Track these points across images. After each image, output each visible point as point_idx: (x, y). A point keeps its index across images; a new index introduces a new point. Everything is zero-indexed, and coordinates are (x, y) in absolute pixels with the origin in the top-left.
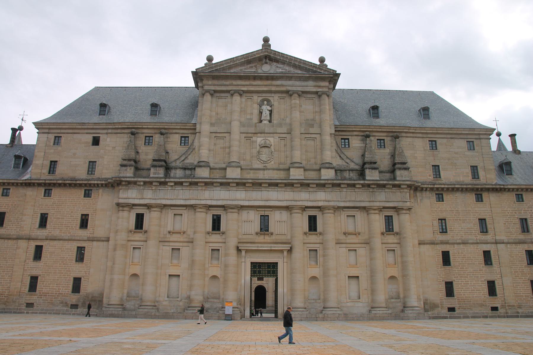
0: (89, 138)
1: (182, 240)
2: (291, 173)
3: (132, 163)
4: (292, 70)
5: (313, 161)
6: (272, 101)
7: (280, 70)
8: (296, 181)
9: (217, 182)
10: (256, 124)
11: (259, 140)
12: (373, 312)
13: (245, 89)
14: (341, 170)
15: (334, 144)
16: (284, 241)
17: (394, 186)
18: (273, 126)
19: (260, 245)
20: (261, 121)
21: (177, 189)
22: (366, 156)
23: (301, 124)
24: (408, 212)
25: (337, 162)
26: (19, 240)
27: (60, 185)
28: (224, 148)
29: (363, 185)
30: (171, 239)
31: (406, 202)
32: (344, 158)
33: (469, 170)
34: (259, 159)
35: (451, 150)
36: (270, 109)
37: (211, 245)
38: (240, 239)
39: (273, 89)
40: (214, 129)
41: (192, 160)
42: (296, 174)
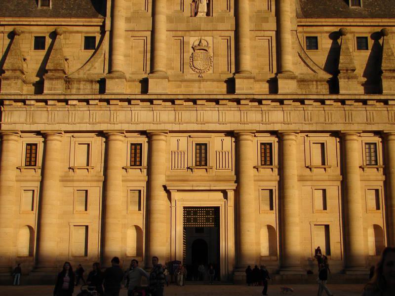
1: (89, 178)
2: (237, 86)
3: (18, 73)
8: (244, 97)
10: (188, 17)
12: (348, 273)
15: (297, 45)
17: (379, 101)
18: (212, 21)
19: (194, 183)
20: (196, 14)
21: (81, 109)
22: (341, 61)
23: (250, 18)
30: (75, 178)
32: (310, 64)
34: (193, 67)
37: (129, 184)
38: (168, 176)
40: (132, 26)
41: (98, 69)
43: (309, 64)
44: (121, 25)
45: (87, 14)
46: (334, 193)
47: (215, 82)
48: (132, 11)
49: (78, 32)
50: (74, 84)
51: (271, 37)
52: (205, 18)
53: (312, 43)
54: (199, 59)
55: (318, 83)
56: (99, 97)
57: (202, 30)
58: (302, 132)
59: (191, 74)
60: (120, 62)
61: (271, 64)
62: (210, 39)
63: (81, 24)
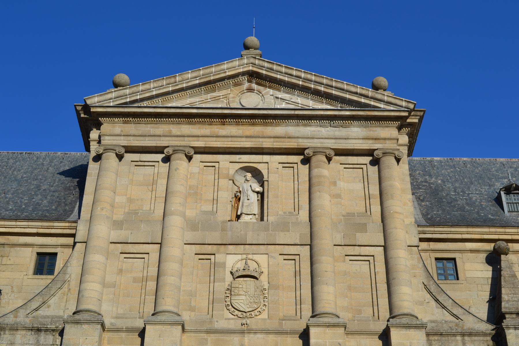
4: (310, 103)
5: (368, 311)
7: (284, 106)
10: (224, 222)
11: (233, 261)
13: (200, 143)
14: (441, 334)
18: (266, 229)
25: (430, 313)
32: (448, 303)
36: (259, 189)
39: (267, 144)
43: (445, 304)
44: (103, 232)
45: (46, 216)
47: (270, 336)
48: (127, 211)
50: (4, 334)
51: (373, 256)
52: (254, 223)
53: (448, 267)
54: (241, 293)
55: (466, 338)
57: (248, 243)
59: (226, 319)
61: (374, 304)
62: (262, 260)
63: (34, 231)
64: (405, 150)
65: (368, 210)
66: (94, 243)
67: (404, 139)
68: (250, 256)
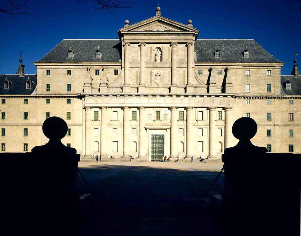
0: (66, 71)
3: (90, 85)
6: (162, 49)
8: (174, 94)
9: (134, 95)
11: (155, 71)
13: (147, 41)
15: (194, 73)
16: (166, 124)
17: (224, 96)
18: (162, 64)
20: (156, 61)
24: (230, 109)
26: (37, 126)
27: (53, 97)
28: (137, 76)
29: (208, 96)
31: (230, 104)
33: (266, 87)
35: (258, 76)
36: (160, 53)
39: (162, 41)
40: (132, 65)
41: (121, 83)
42: (174, 90)
44: (128, 65)
46: (206, 130)
49: (111, 68)
53: (200, 72)
56: (120, 94)
58: (195, 107)
60: (128, 81)
62: (161, 71)
64: (194, 42)
65: (184, 58)
66: (126, 68)
67: (194, 38)
68: (159, 70)
